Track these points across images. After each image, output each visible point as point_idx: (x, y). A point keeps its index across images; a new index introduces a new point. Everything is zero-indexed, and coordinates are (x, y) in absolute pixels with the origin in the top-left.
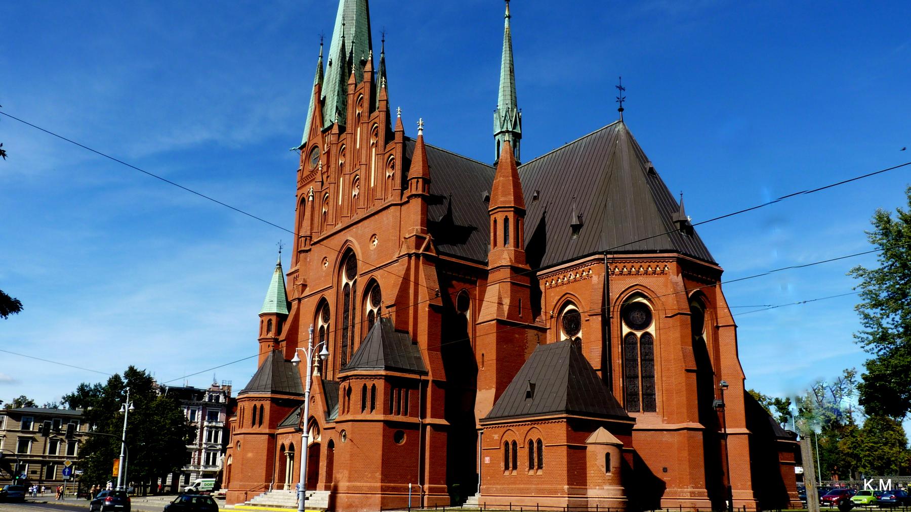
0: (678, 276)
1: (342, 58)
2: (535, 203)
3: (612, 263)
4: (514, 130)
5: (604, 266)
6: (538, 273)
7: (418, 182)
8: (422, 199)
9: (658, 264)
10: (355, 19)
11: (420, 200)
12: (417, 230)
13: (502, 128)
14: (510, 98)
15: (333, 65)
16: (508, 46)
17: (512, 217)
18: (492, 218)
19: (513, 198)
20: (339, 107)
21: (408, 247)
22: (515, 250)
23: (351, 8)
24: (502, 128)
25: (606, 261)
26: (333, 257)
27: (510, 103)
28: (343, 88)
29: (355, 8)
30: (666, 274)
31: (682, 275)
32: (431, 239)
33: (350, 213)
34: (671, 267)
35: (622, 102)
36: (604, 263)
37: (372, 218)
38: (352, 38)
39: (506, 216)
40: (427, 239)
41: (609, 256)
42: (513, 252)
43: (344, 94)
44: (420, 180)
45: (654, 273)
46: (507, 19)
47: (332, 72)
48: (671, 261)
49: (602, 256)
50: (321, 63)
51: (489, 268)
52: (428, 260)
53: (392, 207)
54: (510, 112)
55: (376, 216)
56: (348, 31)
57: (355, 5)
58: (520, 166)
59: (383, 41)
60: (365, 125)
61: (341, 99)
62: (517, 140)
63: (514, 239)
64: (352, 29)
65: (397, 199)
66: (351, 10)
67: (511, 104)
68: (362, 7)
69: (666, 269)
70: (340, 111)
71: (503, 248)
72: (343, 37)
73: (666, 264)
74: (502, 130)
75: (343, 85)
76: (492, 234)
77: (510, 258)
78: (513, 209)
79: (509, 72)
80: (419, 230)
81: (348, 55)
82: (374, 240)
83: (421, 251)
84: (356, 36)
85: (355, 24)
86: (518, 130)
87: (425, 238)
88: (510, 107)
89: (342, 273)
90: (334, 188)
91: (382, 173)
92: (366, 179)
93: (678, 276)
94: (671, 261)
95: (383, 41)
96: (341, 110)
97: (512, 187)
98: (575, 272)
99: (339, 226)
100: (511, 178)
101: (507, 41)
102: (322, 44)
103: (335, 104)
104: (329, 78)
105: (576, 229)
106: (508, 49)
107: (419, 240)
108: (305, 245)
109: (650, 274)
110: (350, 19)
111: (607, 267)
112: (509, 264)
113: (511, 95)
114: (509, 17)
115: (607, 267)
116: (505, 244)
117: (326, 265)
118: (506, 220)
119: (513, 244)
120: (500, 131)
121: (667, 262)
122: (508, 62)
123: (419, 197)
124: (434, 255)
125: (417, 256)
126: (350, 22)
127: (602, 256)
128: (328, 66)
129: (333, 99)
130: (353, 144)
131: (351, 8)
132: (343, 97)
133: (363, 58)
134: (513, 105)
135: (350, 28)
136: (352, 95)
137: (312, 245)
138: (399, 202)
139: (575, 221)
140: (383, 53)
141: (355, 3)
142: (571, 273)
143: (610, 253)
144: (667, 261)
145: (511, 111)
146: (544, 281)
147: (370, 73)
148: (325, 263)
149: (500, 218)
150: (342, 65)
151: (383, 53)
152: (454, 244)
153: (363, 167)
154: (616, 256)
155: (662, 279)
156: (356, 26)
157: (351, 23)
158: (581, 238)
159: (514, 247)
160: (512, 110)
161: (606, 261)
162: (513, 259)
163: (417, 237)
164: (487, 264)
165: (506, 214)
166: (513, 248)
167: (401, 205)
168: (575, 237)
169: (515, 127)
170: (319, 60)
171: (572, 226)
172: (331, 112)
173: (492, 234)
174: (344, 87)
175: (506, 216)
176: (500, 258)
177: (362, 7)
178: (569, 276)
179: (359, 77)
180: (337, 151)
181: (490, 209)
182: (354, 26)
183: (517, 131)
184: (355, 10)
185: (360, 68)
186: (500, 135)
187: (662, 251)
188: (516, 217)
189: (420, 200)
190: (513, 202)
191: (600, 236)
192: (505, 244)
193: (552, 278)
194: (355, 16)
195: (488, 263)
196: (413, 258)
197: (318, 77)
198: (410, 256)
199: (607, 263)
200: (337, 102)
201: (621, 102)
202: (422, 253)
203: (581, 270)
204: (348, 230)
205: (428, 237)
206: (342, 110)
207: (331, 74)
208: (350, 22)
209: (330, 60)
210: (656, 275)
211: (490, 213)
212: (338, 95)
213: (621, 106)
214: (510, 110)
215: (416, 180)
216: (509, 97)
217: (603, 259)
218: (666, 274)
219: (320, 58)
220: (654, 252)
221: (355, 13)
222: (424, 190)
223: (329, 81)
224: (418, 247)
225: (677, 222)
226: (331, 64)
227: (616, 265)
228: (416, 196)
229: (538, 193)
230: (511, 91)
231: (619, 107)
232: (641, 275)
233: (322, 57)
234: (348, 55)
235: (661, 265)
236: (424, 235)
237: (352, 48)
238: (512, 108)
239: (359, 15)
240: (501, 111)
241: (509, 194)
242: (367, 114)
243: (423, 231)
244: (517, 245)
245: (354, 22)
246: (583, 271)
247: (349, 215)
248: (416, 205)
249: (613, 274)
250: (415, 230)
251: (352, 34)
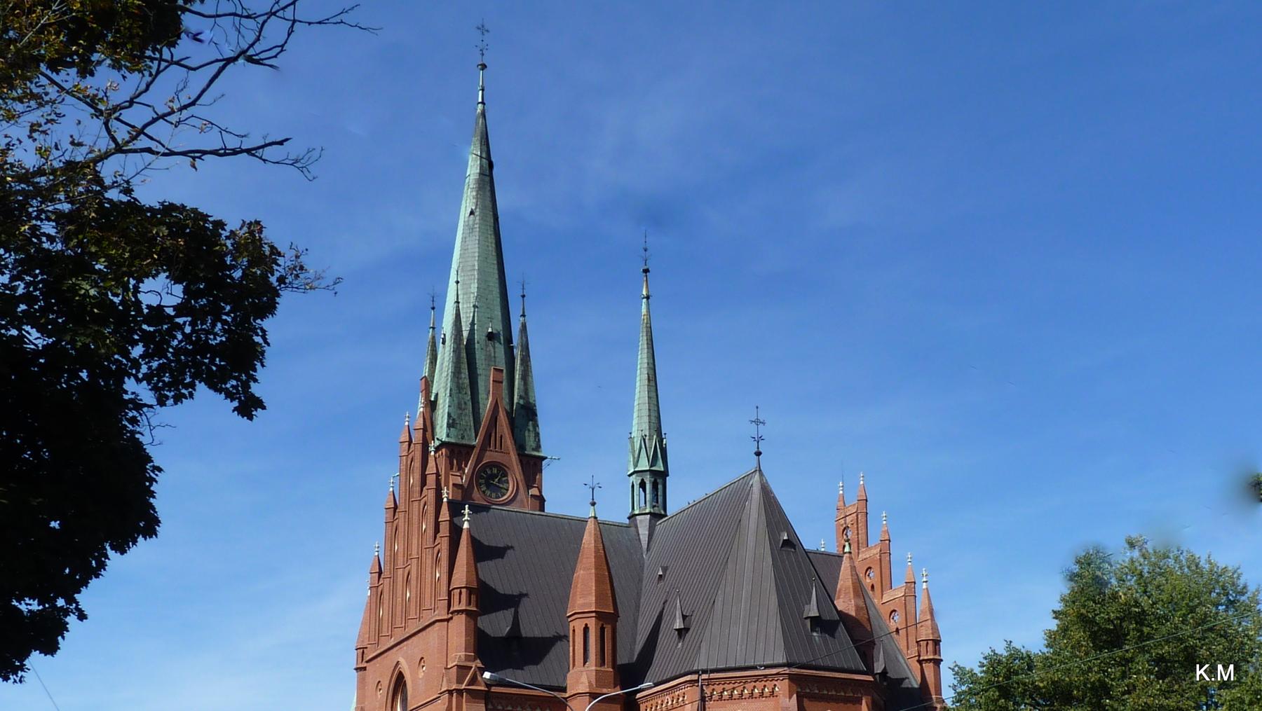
0: (790, 698)
1: (456, 336)
2: (662, 583)
3: (708, 685)
4: (653, 468)
5: (698, 689)
6: (639, 696)
7: (460, 593)
8: (466, 614)
9: (766, 683)
10: (477, 268)
11: (464, 616)
12: (460, 657)
13: (636, 466)
14: (647, 421)
15: (446, 343)
16: (646, 342)
17: (594, 626)
18: (571, 625)
19: (594, 599)
20: (452, 415)
21: (449, 681)
22: (596, 670)
23: (470, 251)
24: (636, 465)
25: (700, 684)
26: (387, 682)
27: (648, 428)
28: (458, 383)
29: (477, 250)
30: (777, 696)
31: (797, 696)
32: (479, 668)
33: (404, 622)
34: (782, 686)
35: (761, 442)
36: (698, 686)
37: (420, 635)
38: (472, 300)
39: (586, 625)
40: (473, 669)
41: (705, 676)
42: (594, 674)
43: (460, 393)
44: (464, 591)
45: (762, 695)
46: (645, 300)
47: (446, 355)
48: (781, 678)
49: (695, 677)
50: (433, 338)
51: (567, 695)
52: (474, 695)
53: (437, 624)
54: (647, 441)
55: (424, 633)
56: (467, 288)
57: (477, 246)
58: (666, 518)
59: (523, 296)
60: (416, 504)
61: (456, 402)
62: (658, 481)
63: (596, 655)
64: (472, 285)
65: (442, 612)
66: (470, 255)
67: (650, 429)
68: (488, 246)
69: (777, 689)
70: (454, 420)
71: (582, 669)
72: (457, 302)
73: (776, 683)
74: (637, 469)
75: (458, 378)
76: (571, 648)
77: (590, 682)
78: (594, 614)
79: (647, 381)
80: (463, 657)
81: (465, 334)
82: (423, 664)
83: (463, 687)
84: (479, 297)
85: (476, 277)
86: (660, 467)
87: (472, 667)
88: (648, 435)
89: (396, 705)
90: (390, 584)
91: (432, 573)
92: (417, 578)
93: (790, 698)
94: (781, 678)
95: (523, 296)
96: (455, 417)
97: (594, 584)
98: (671, 695)
99: (392, 642)
100: (593, 571)
101: (645, 334)
102: (433, 308)
103: (447, 411)
104: (442, 364)
105: (682, 633)
106: (646, 346)
107: (463, 669)
108: (460, 602)
109: (756, 698)
110: (469, 268)
111: (702, 690)
112: (587, 690)
113: (649, 416)
114: (648, 298)
115: (702, 690)
116: (584, 664)
117: (424, 668)
118: (586, 629)
119: (594, 662)
120: (632, 471)
121: (777, 680)
122: (646, 365)
123: (463, 613)
124: (483, 688)
125: (460, 692)
126: (469, 273)
127: (695, 677)
128: (441, 345)
129: (445, 401)
130: (407, 526)
131: (470, 251)
132: (458, 398)
133: (490, 330)
134: (652, 430)
135: (471, 283)
136: (405, 457)
137: (367, 662)
138: (446, 617)
139: (678, 624)
140: (523, 315)
141: (477, 242)
142: (667, 697)
143: (705, 672)
144: (776, 679)
145: (649, 439)
146: (645, 705)
147: (422, 431)
148: (423, 667)
149: (578, 626)
150: (455, 347)
151: (523, 315)
152: (519, 666)
153: (415, 561)
154: (712, 676)
155: (770, 703)
156: (478, 280)
157: (472, 275)
158: (685, 647)
159: (596, 666)
160: (651, 438)
161: (700, 684)
162: (594, 683)
163: (459, 667)
164: (564, 690)
165: (586, 621)
166: (594, 668)
167: (448, 620)
168: (680, 644)
169: (653, 462)
170: (430, 334)
171: (676, 630)
172: (442, 422)
173: (571, 648)
174: (460, 382)
175: (586, 625)
176: (577, 682)
177: (488, 246)
178: (666, 701)
179: (485, 360)
180: (392, 532)
181: (568, 615)
182: (476, 281)
183: (659, 469)
184: (477, 254)
185: (487, 346)
186: (634, 476)
187: (767, 667)
188: (601, 623)
189: (464, 616)
190: (594, 605)
191: (700, 647)
192: (584, 664)
193: (651, 702)
194: (476, 263)
195: (566, 688)
196: (455, 694)
197: (428, 361)
198: (450, 692)
199: (702, 685)
200: (449, 406)
201: (758, 442)
202: (464, 689)
203: (677, 693)
204: (398, 647)
205: (474, 666)
206: (459, 417)
207: (444, 359)
208: (469, 273)
209: (442, 336)
210: (764, 699)
211: (569, 620)
212: (450, 396)
213: (758, 448)
214: (647, 438)
215: (459, 590)
216: (646, 419)
217: (697, 681)
218: (777, 696)
219: (431, 330)
220: (754, 668)
221: (477, 258)
222: (469, 603)
223: (442, 369)
224: (460, 681)
225: (806, 618)
226: (444, 343)
227: (713, 687)
228: (458, 612)
229: (665, 569)
230: (649, 410)
231: (756, 450)
232: (745, 698)
233: (433, 328)
234: (465, 334)
235: (770, 684)
236: (469, 664)
237: (474, 316)
238: (650, 436)
239: (483, 259)
240: (635, 440)
241: (590, 594)
242: (418, 489)
243: (467, 658)
244: (602, 661)
245: (476, 273)
246: (679, 695)
247: (403, 625)
248: (460, 623)
249: (711, 700)
250: (458, 657)
251: (474, 293)
